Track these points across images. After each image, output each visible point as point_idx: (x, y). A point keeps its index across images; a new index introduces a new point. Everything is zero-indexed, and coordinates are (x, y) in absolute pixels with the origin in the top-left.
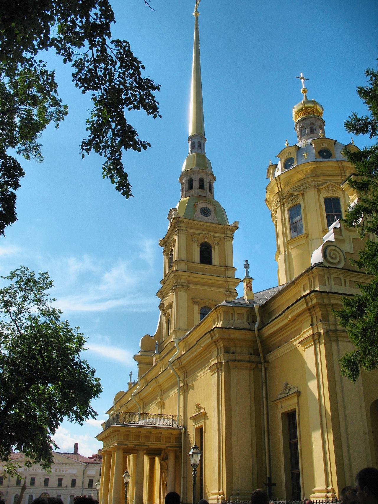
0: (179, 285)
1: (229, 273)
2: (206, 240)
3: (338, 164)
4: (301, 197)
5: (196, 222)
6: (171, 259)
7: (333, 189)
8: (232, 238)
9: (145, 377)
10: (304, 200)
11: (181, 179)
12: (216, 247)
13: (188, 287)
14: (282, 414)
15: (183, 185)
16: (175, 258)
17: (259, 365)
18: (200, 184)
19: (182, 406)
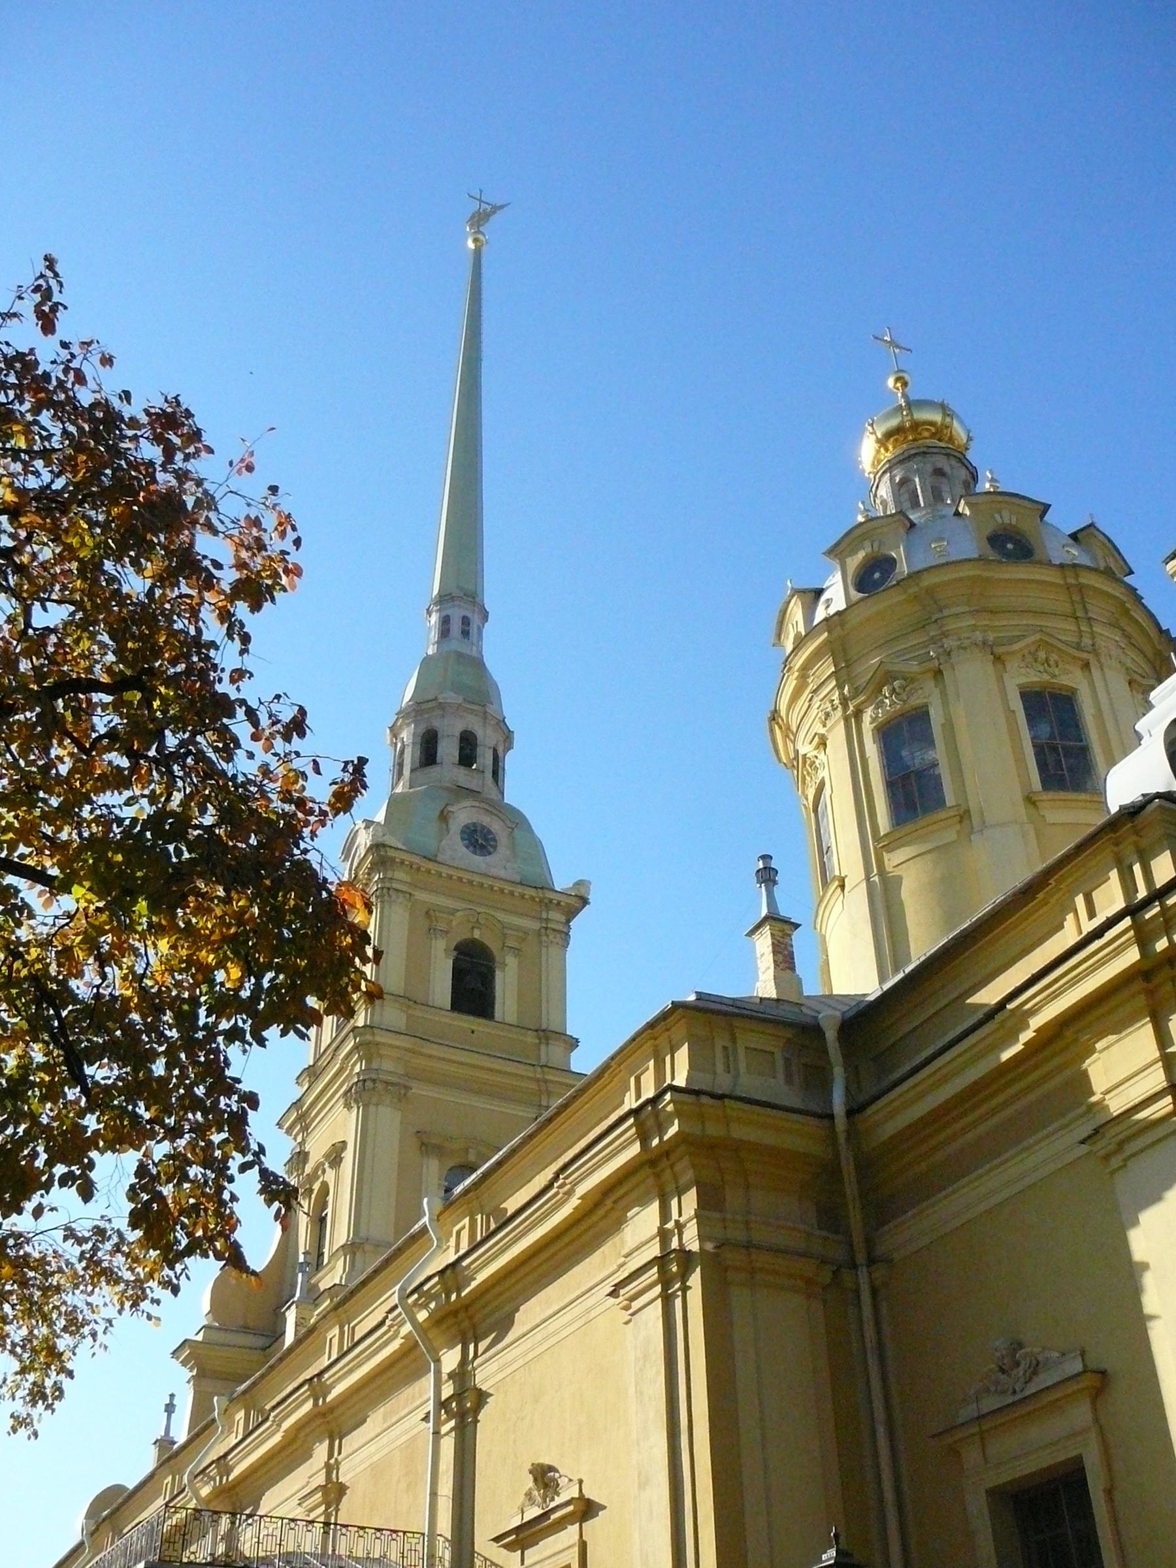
0: (374, 1081)
1: (553, 1053)
2: (477, 934)
3: (1065, 578)
4: (932, 683)
5: (445, 871)
7: (1054, 657)
8: (566, 936)
9: (247, 1396)
10: (944, 694)
12: (511, 961)
13: (407, 1088)
14: (992, 1493)
15: (402, 752)
17: (847, 1277)
18: (461, 749)
19: (446, 1487)
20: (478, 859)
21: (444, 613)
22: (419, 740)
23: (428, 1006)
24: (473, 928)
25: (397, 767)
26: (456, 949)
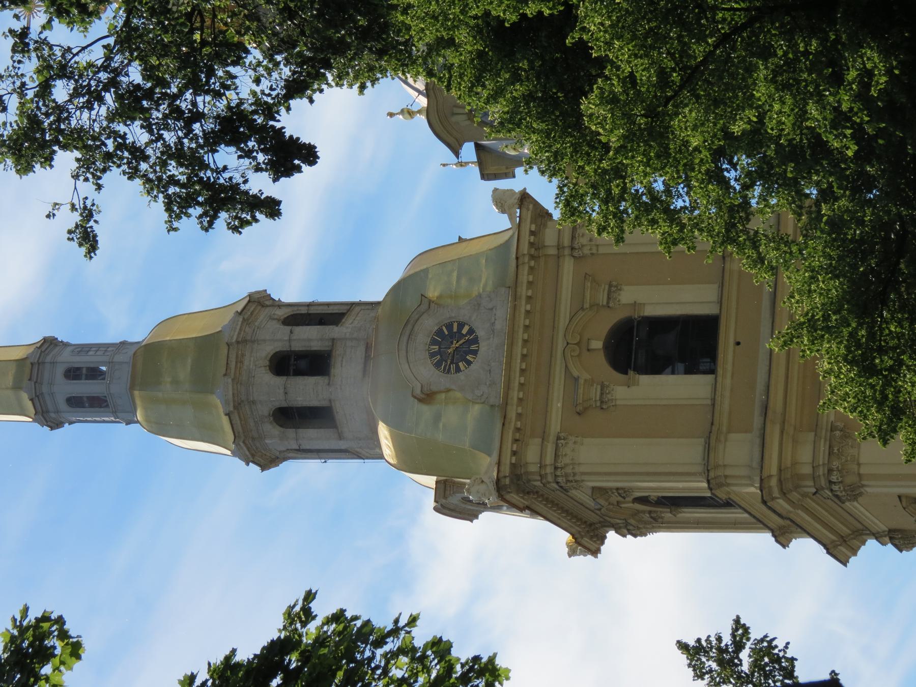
0: (830, 471)
2: (598, 344)
6: (676, 502)
11: (267, 461)
12: (628, 295)
13: (833, 429)
18: (299, 373)
20: (484, 348)
21: (63, 406)
22: (291, 432)
23: (713, 405)
24: (588, 350)
25: (322, 455)
26: (626, 373)
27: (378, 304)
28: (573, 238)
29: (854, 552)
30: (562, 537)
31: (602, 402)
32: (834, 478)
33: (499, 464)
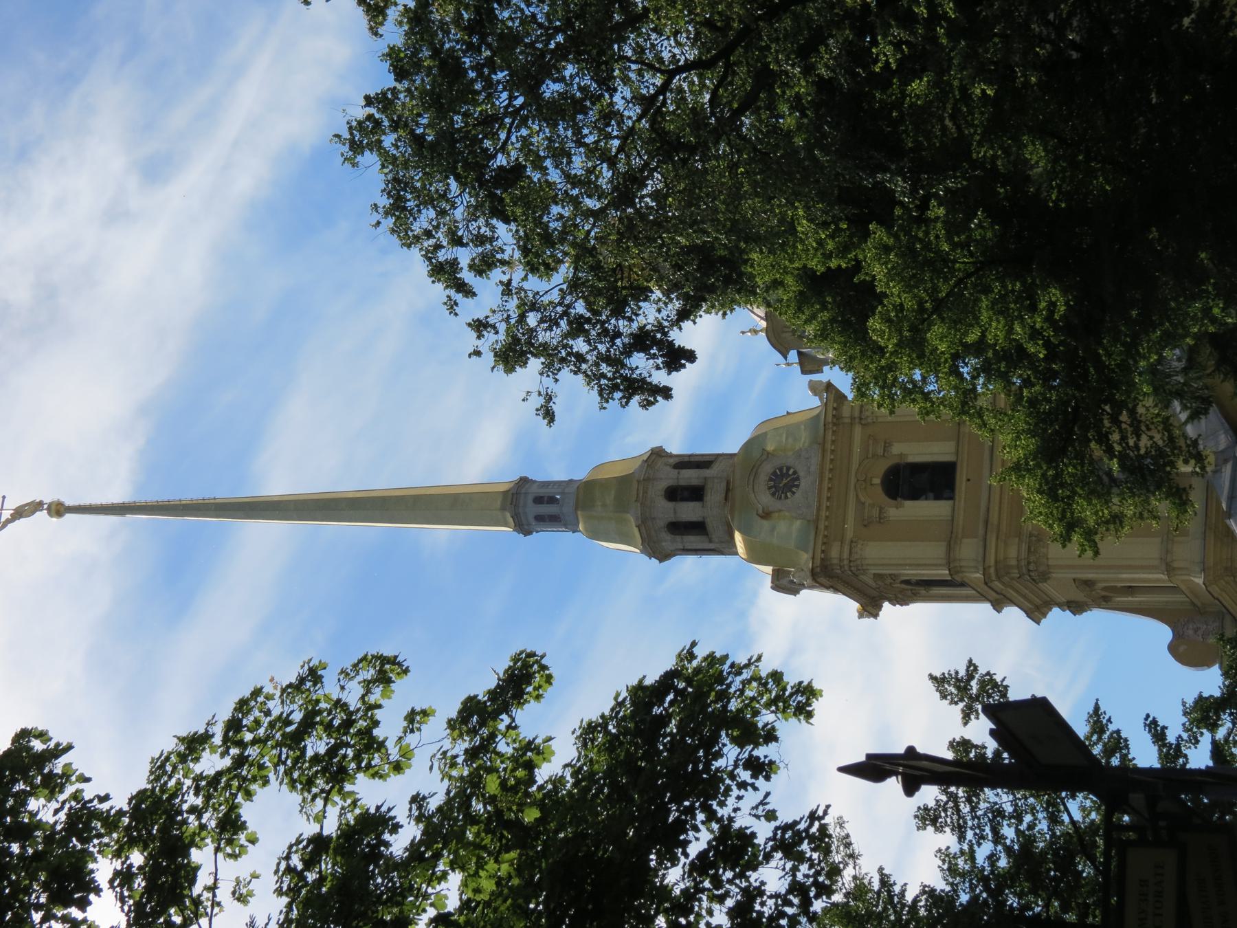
0: (1029, 563)
2: (877, 481)
6: (929, 584)
11: (663, 556)
12: (897, 449)
13: (1031, 535)
16: (943, 573)
18: (684, 499)
20: (804, 483)
21: (533, 522)
22: (678, 538)
27: (734, 455)
28: (861, 412)
29: (1045, 615)
30: (853, 606)
31: (880, 518)
32: (1031, 568)
33: (813, 558)
